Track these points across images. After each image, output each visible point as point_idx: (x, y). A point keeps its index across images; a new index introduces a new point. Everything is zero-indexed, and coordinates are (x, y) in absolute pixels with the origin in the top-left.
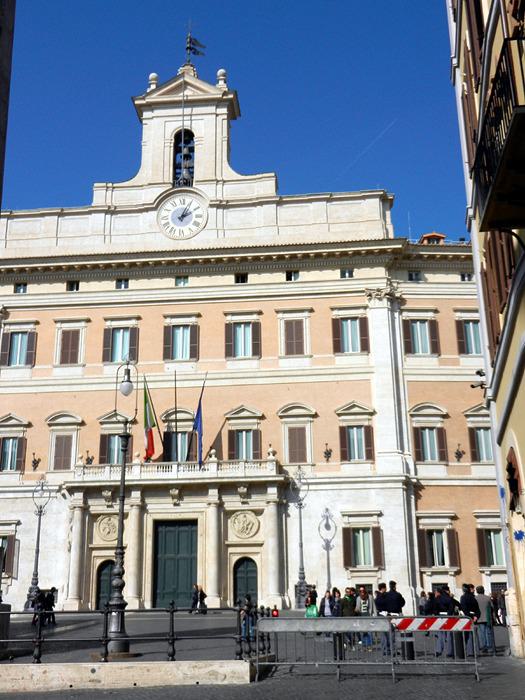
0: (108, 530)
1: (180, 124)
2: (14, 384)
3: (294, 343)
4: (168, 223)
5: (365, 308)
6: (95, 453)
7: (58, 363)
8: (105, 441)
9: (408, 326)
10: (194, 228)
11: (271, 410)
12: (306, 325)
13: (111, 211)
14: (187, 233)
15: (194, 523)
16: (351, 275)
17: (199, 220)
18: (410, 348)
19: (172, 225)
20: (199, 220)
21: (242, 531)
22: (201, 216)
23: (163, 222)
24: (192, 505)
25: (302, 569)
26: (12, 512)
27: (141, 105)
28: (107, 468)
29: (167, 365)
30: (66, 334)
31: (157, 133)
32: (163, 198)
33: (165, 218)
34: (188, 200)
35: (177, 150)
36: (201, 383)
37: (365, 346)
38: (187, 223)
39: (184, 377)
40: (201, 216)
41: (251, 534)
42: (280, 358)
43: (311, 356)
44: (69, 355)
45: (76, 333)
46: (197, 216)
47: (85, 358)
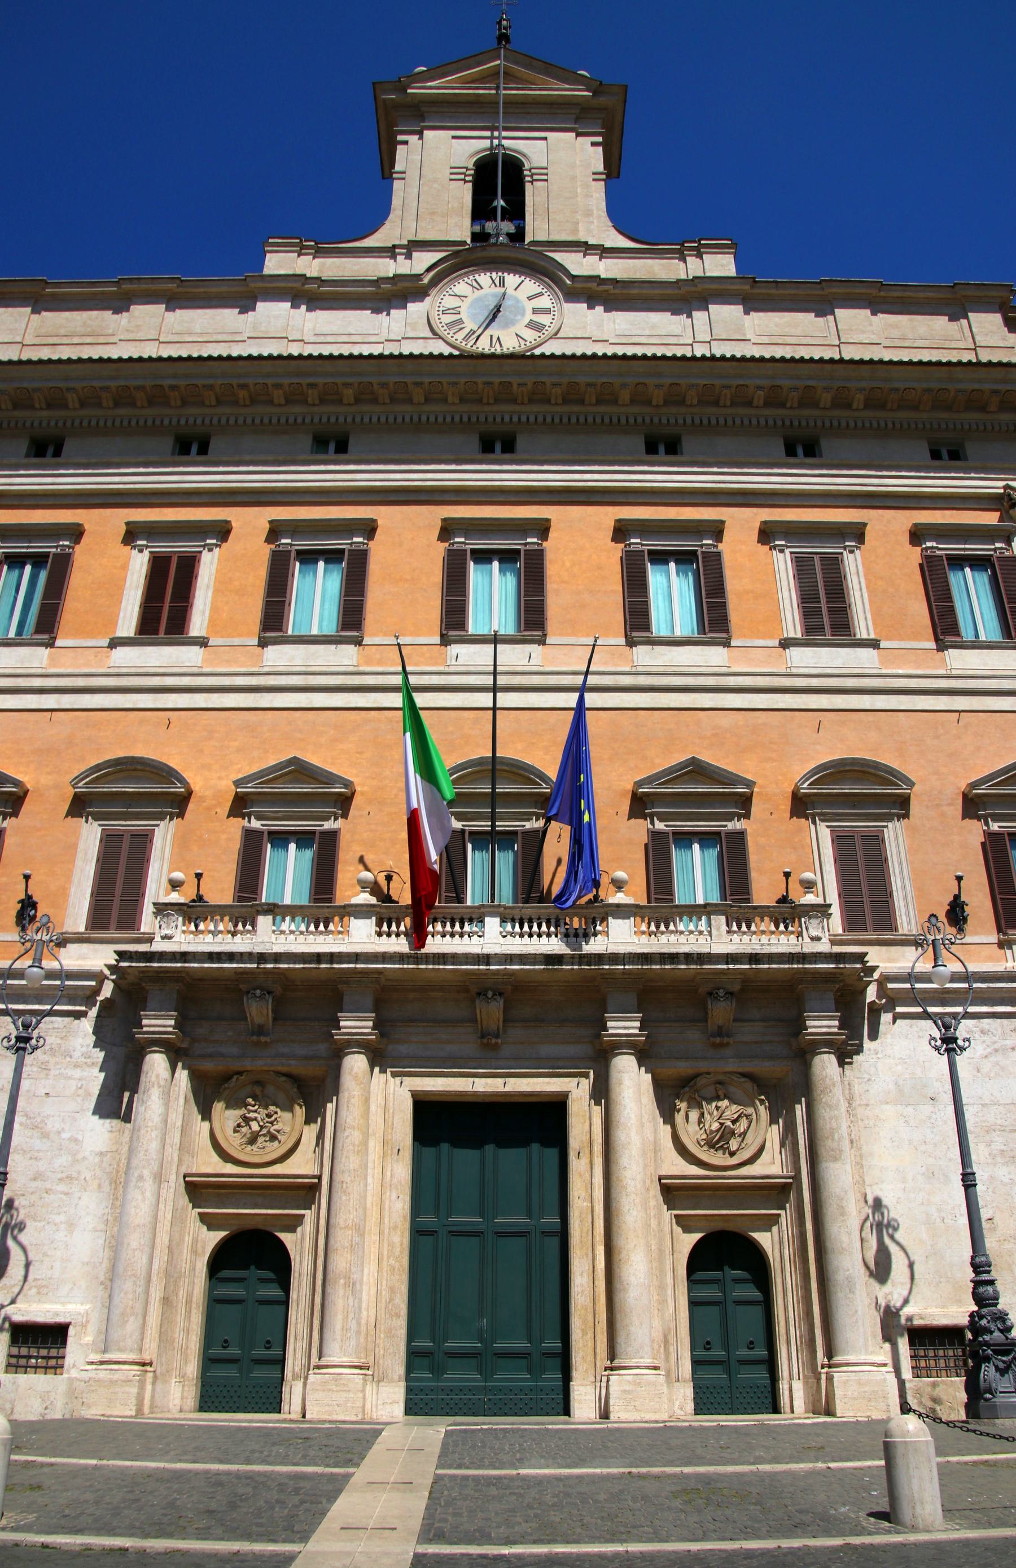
0: (255, 1126)
3: (826, 614)
6: (221, 890)
8: (252, 849)
10: (530, 335)
11: (776, 774)
12: (854, 565)
17: (544, 319)
20: (544, 319)
21: (719, 1140)
22: (547, 311)
23: (448, 319)
25: (980, 1266)
27: (396, 106)
28: (264, 922)
29: (455, 649)
30: (158, 566)
31: (433, 173)
33: (456, 311)
34: (511, 280)
35: (481, 211)
38: (513, 323)
39: (517, 680)
40: (547, 311)
41: (745, 1155)
42: (786, 644)
43: (874, 644)
44: (165, 612)
45: (189, 565)
46: (536, 311)
47: (212, 622)
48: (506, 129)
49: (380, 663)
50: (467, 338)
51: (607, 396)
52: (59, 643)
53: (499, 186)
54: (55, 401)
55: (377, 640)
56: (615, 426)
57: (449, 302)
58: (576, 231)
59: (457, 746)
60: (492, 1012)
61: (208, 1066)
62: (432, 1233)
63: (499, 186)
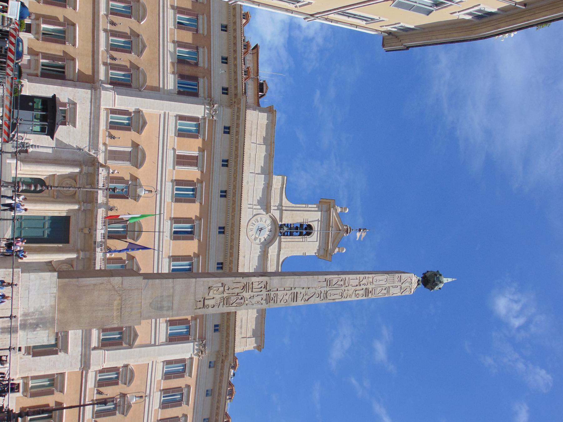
1: (316, 230)
2: (166, 124)
4: (258, 222)
5: (195, 339)
7: (177, 153)
9: (183, 361)
10: (253, 237)
13: (268, 187)
14: (250, 233)
15: (68, 242)
16: (216, 330)
18: (168, 363)
19: (256, 224)
23: (259, 219)
24: (79, 241)
26: (82, 124)
32: (274, 221)
33: (261, 220)
36: (156, 248)
37: (173, 339)
48: (320, 233)
49: (167, 207)
50: (253, 223)
51: (231, 255)
52: (176, 138)
53: (305, 230)
54: (237, 132)
55: (173, 206)
56: (225, 256)
57: (264, 220)
58: (285, 248)
59: (146, 224)
60: (86, 231)
61: (78, 178)
62: (44, 219)
63: (305, 230)
